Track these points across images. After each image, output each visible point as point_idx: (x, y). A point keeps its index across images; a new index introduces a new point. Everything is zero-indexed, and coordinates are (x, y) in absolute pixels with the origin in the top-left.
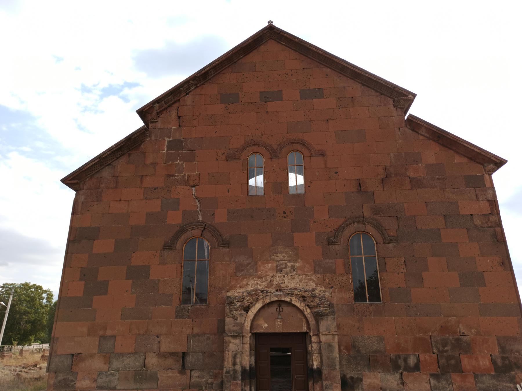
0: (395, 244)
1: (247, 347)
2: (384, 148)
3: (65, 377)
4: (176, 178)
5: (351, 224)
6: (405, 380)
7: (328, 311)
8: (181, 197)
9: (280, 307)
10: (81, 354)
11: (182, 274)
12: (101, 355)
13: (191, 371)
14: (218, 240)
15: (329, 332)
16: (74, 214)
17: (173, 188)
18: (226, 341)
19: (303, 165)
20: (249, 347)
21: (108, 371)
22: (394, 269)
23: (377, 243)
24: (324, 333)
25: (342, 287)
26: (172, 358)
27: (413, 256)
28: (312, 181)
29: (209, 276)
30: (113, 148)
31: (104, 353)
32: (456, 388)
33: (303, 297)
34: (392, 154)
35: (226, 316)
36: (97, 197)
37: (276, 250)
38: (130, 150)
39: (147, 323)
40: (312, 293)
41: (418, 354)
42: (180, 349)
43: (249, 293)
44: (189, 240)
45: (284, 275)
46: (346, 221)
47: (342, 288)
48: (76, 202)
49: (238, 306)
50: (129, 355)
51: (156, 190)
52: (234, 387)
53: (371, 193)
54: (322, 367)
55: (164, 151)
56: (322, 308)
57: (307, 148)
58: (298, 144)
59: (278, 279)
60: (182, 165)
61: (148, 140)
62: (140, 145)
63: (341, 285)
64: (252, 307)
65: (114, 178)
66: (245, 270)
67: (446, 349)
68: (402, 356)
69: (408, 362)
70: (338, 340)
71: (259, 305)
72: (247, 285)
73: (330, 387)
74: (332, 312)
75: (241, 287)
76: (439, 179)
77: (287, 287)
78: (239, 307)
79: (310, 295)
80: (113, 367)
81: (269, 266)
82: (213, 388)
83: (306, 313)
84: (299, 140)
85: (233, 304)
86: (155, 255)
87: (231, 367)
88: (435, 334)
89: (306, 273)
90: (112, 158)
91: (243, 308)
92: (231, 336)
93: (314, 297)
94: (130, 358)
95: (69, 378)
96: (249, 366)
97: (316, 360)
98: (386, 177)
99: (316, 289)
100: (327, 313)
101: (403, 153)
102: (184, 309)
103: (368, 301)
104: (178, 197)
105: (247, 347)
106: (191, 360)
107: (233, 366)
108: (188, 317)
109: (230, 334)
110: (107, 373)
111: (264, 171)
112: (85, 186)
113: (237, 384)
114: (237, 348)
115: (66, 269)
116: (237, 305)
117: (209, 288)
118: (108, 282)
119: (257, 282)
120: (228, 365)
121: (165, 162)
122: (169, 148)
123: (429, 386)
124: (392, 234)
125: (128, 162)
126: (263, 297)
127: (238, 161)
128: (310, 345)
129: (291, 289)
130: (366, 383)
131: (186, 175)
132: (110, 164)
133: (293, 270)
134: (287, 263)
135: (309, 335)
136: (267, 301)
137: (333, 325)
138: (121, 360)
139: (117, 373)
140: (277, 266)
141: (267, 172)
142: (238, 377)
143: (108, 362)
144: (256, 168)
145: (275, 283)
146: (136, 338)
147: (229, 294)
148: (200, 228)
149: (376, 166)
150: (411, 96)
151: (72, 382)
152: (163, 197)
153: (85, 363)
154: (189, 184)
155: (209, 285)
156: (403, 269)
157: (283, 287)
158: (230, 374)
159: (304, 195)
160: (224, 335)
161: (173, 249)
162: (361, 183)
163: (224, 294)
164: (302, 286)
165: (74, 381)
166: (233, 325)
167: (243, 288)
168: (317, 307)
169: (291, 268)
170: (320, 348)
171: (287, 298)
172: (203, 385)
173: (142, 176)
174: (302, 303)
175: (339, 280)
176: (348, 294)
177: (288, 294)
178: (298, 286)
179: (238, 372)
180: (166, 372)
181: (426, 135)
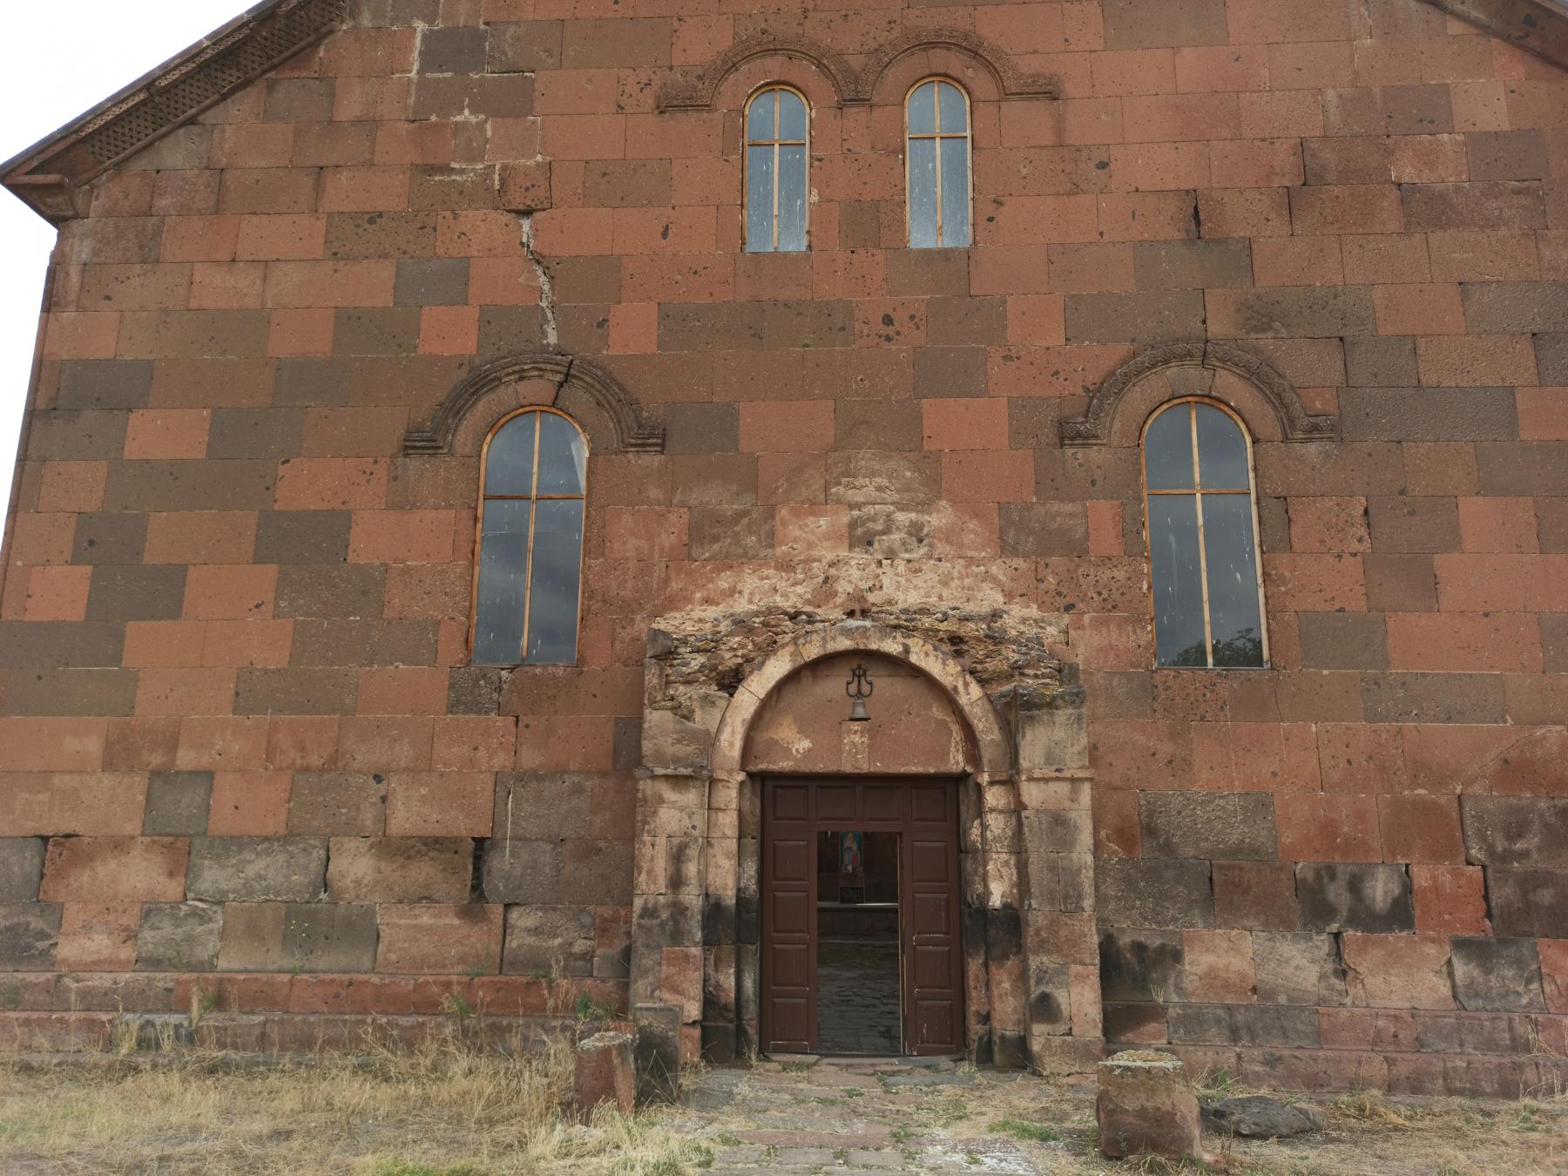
0: (1329, 446)
1: (727, 821)
2: (1300, 69)
3: (15, 920)
4: (458, 178)
5: (1154, 366)
6: (1349, 958)
7: (1056, 689)
8: (475, 253)
9: (859, 677)
10: (77, 836)
11: (478, 547)
12: (154, 842)
13: (508, 907)
14: (619, 421)
15: (1057, 770)
16: (53, 309)
17: (444, 218)
18: (644, 797)
19: (968, 134)
20: (736, 823)
21: (181, 902)
22: (1322, 542)
23: (1255, 442)
24: (1037, 774)
25: (1110, 606)
26: (432, 859)
27: (1402, 492)
28: (1001, 199)
29: (584, 557)
30: (203, 51)
31: (167, 835)
32: (1556, 994)
33: (955, 640)
34: (1331, 95)
35: (646, 702)
36: (142, 247)
37: (852, 466)
38: (273, 67)
39: (336, 728)
40: (989, 628)
41: (1407, 865)
42: (463, 826)
43: (741, 625)
44: (504, 420)
45: (880, 557)
46: (1135, 354)
47: (1109, 611)
48: (58, 264)
49: (696, 668)
50: (265, 845)
51: (375, 222)
52: (673, 970)
53: (1240, 246)
54: (1026, 902)
55: (411, 71)
56: (1030, 681)
57: (988, 65)
58: (949, 49)
59: (855, 574)
60: (480, 127)
61: (345, 27)
62: (314, 46)
63: (1104, 600)
64: (751, 673)
65: (208, 173)
66: (725, 538)
67: (1518, 846)
68: (1340, 869)
69: (1368, 892)
70: (1093, 798)
71: (777, 667)
72: (733, 592)
73: (1054, 980)
74: (1072, 694)
75: (707, 601)
76: (1518, 192)
77: (890, 602)
78: (699, 671)
79: (981, 632)
80: (202, 889)
81: (822, 522)
82: (591, 975)
83: (963, 700)
84: (955, 34)
85: (676, 662)
86: (372, 474)
87: (661, 894)
88: (1477, 789)
89: (970, 553)
90: (199, 95)
91: (714, 674)
92: (666, 777)
93: (996, 639)
94: (268, 855)
95: (28, 924)
96: (734, 891)
97: (1001, 877)
98: (1304, 184)
99: (1006, 612)
100: (1054, 698)
101: (1377, 90)
102: (484, 676)
103: (1210, 660)
104: (463, 254)
105: (728, 822)
106: (507, 868)
107: (669, 892)
108: (500, 709)
109: (660, 771)
110: (179, 909)
111: (811, 157)
112: (94, 203)
113: (687, 957)
114: (686, 821)
115: (18, 519)
116: (693, 663)
117: (583, 604)
118: (186, 571)
119: (774, 581)
120: (651, 884)
121: (411, 118)
122: (430, 60)
123: (1448, 984)
124: (1318, 405)
125: (265, 112)
126: (795, 639)
127: (706, 115)
128: (977, 823)
129: (905, 611)
130: (1194, 969)
131: (498, 167)
132: (192, 121)
133: (914, 539)
134: (894, 512)
135: (972, 784)
136: (812, 651)
137: (1073, 745)
138: (234, 861)
139: (219, 912)
140: (853, 525)
141: (820, 160)
142: (689, 932)
143: (183, 869)
144: (777, 146)
145: (843, 588)
146: (293, 780)
147: (661, 624)
148: (549, 376)
149: (1263, 140)
151: (38, 940)
152: (404, 253)
153: (92, 869)
154: (510, 202)
155: (584, 593)
156: (1360, 540)
157: (873, 604)
158: (659, 920)
159: (968, 255)
160: (638, 772)
161: (441, 451)
162: (1200, 207)
163: (643, 625)
164: (949, 599)
165: (48, 937)
166: (675, 736)
167: (717, 604)
168: (1009, 677)
169: (910, 534)
170: (1019, 833)
171: (890, 641)
172: (553, 963)
173: (321, 168)
174: (951, 662)
175: (1097, 581)
176: (1135, 632)
177: (896, 627)
178: (935, 599)
179: (689, 913)
180: (410, 910)
181: (1476, 14)
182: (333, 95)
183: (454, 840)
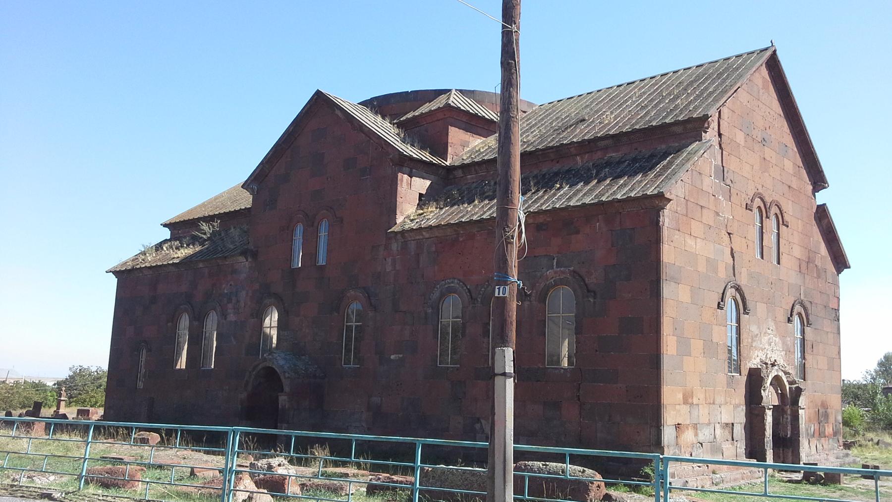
3: (674, 451)
24: (802, 407)
34: (811, 239)
65: (685, 201)
75: (755, 359)
136: (773, 376)
140: (769, 339)
150: (827, 185)
181: (824, 227)
182: (702, 180)
183: (729, 424)
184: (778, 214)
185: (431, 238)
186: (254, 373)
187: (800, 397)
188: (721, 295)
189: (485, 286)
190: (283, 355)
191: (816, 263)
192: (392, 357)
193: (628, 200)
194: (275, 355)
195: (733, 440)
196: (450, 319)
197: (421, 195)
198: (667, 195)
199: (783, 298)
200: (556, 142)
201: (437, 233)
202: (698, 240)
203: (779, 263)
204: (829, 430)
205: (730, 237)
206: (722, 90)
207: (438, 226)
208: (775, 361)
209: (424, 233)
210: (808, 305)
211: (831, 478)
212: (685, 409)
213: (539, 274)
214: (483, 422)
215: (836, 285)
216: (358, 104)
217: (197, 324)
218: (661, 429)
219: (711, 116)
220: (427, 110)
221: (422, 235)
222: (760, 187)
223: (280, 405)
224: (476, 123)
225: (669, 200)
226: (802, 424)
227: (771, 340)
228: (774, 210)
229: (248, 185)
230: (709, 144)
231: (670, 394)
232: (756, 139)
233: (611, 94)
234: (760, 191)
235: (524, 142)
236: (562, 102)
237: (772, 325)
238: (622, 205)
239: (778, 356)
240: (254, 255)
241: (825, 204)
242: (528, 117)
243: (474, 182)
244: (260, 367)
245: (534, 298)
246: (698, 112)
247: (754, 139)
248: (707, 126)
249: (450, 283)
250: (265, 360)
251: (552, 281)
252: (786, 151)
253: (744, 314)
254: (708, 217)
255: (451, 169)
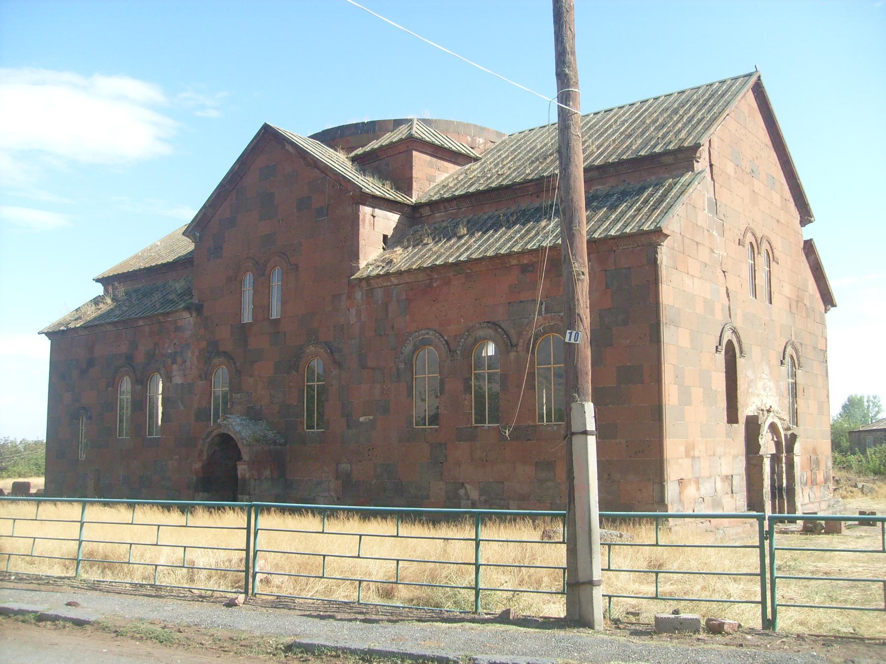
24: (797, 455)
42: (729, 473)
75: (751, 406)
140: (764, 385)
145: (764, 403)
183: (729, 476)
184: (769, 251)
185: (400, 285)
186: (208, 440)
187: (795, 443)
188: (719, 338)
189: (465, 337)
190: (238, 420)
191: (805, 301)
192: (362, 419)
193: (622, 237)
194: (230, 419)
195: (732, 493)
196: (426, 374)
197: (385, 237)
198: (665, 231)
199: (776, 340)
200: (535, 174)
201: (406, 278)
202: (696, 280)
203: (771, 303)
204: (820, 477)
205: (725, 276)
206: (711, 117)
207: (409, 271)
208: (771, 407)
209: (392, 279)
210: (799, 347)
211: (832, 526)
212: (686, 462)
213: (526, 321)
214: (466, 485)
215: (823, 323)
216: (308, 137)
217: (139, 387)
218: (664, 486)
219: (703, 145)
220: (387, 142)
221: (391, 282)
222: (750, 222)
223: (239, 475)
224: (442, 155)
225: (666, 236)
226: (797, 473)
227: (766, 386)
228: (765, 246)
229: (190, 232)
230: (702, 175)
231: (673, 448)
232: (745, 170)
233: (588, 122)
234: (751, 226)
235: (499, 175)
236: (534, 131)
237: (766, 368)
238: (616, 243)
239: (772, 401)
240: (198, 309)
241: (811, 240)
242: (498, 148)
243: (443, 221)
244: (215, 433)
245: (521, 348)
246: (689, 141)
247: (743, 170)
248: (699, 155)
249: (424, 335)
250: (220, 426)
251: (541, 328)
252: (774, 184)
253: (740, 357)
254: (703, 254)
255: (417, 207)
